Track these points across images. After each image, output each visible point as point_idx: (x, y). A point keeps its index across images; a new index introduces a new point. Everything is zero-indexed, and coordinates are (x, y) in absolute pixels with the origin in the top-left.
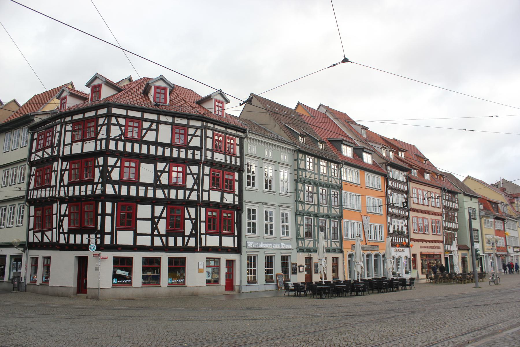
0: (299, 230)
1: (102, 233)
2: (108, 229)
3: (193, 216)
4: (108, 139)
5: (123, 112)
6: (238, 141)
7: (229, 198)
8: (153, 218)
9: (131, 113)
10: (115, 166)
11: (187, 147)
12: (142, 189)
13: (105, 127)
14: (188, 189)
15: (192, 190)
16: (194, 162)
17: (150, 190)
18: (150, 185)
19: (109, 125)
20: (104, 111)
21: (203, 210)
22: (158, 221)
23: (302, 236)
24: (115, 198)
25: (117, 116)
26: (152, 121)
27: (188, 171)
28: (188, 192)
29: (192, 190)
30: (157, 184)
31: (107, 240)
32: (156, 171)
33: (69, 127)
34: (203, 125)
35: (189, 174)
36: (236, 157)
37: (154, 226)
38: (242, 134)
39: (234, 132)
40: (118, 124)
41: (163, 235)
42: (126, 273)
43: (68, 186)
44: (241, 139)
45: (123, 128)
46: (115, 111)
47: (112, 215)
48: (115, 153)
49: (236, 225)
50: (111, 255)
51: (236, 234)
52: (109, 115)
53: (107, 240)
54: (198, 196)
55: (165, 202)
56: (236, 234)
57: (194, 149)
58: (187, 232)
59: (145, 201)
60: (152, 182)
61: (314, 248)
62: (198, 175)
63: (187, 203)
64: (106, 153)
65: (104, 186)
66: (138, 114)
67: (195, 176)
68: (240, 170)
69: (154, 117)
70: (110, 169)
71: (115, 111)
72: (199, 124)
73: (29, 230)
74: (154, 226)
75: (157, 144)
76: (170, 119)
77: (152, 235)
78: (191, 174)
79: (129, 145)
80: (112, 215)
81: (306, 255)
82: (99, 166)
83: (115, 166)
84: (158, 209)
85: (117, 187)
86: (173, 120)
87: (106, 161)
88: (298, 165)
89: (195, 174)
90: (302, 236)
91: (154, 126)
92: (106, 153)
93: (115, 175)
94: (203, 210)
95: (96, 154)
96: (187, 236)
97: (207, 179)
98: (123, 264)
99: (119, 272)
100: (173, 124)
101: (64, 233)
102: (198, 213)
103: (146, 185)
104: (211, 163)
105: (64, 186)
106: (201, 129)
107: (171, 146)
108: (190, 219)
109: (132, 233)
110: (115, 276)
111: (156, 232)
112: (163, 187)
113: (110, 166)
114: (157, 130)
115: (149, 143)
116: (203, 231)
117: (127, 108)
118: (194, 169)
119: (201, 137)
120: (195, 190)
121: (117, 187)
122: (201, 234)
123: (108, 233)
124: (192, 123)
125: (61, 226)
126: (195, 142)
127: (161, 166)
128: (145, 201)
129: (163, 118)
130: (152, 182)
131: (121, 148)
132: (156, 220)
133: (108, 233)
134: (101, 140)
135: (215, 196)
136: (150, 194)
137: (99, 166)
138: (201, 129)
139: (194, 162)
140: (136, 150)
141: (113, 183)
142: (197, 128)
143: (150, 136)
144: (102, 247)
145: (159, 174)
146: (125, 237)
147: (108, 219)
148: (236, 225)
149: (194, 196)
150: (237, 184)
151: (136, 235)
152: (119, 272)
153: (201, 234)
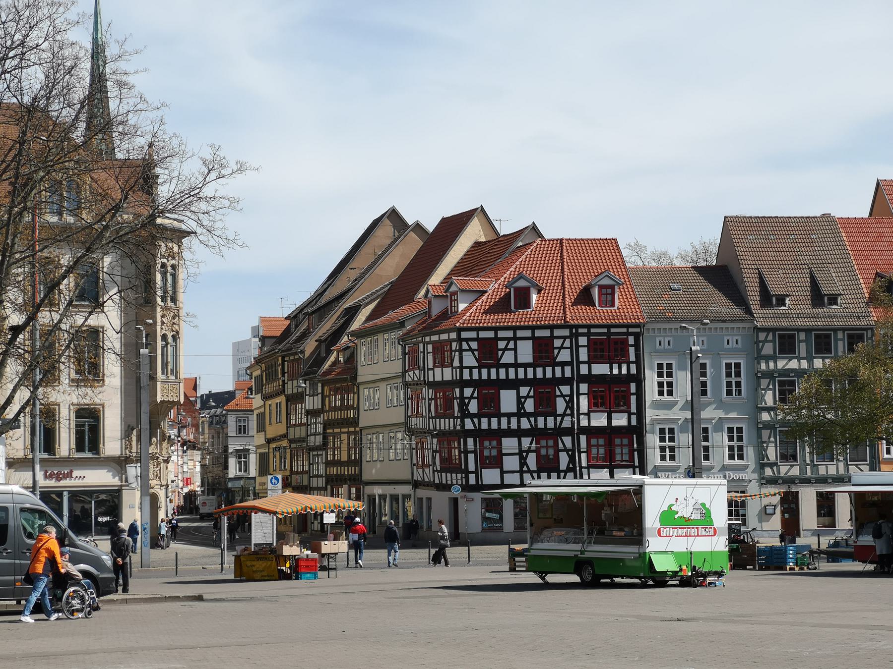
0: (766, 450)
1: (467, 472)
2: (472, 467)
3: (569, 445)
4: (462, 368)
5: (473, 335)
6: (631, 340)
7: (620, 420)
8: (520, 453)
9: (483, 334)
10: (472, 397)
11: (554, 364)
12: (504, 421)
13: (457, 353)
14: (559, 415)
15: (564, 415)
16: (564, 381)
17: (514, 420)
18: (513, 415)
19: (461, 351)
20: (453, 335)
21: (583, 439)
22: (527, 455)
23: (772, 459)
24: (477, 433)
25: (467, 340)
26: (508, 339)
27: (558, 393)
28: (559, 419)
29: (564, 415)
30: (520, 413)
31: (472, 480)
32: (519, 398)
33: (430, 348)
34: (571, 332)
35: (559, 396)
36: (629, 363)
37: (523, 462)
38: (638, 330)
39: (625, 330)
40: (472, 351)
41: (534, 472)
42: (495, 516)
43: (435, 418)
44: (637, 336)
45: (476, 353)
46: (464, 335)
47: (474, 452)
48: (470, 383)
49: (636, 453)
50: (478, 496)
51: (637, 464)
52: (460, 340)
53: (472, 480)
54: (573, 423)
55: (533, 432)
56: (637, 464)
57: (563, 364)
58: (563, 466)
59: (509, 433)
60: (514, 410)
61: (802, 476)
62: (571, 396)
63: (559, 432)
64: (463, 384)
65: (463, 422)
66: (490, 334)
67: (567, 399)
68: (639, 379)
69: (510, 334)
70: (467, 401)
71: (464, 335)
72: (566, 332)
73: (413, 465)
74: (523, 462)
75: (516, 365)
76: (528, 333)
77: (521, 472)
78: (562, 396)
79: (484, 371)
80: (474, 452)
81: (783, 489)
82: (457, 398)
83: (472, 397)
84: (526, 442)
85: (476, 420)
86: (533, 333)
87: (462, 392)
88: (759, 351)
89: (567, 396)
90: (772, 459)
91: (511, 345)
92: (463, 384)
93: (473, 407)
94: (583, 439)
95: (452, 384)
96: (563, 471)
97: (584, 402)
98: (493, 505)
99: (487, 515)
100: (533, 338)
101: (438, 472)
102: (576, 443)
103: (509, 415)
104: (589, 379)
105: (432, 418)
106: (570, 337)
107: (534, 365)
108: (566, 450)
109: (497, 471)
110: (484, 519)
111: (525, 469)
112: (528, 415)
113: (467, 398)
114: (515, 349)
115: (507, 366)
116: (584, 464)
117: (478, 329)
118: (565, 390)
119: (571, 348)
120: (568, 415)
121: (476, 420)
122: (581, 468)
123: (472, 472)
124: (557, 333)
125: (434, 463)
126: (564, 356)
127: (524, 391)
128: (509, 433)
129: (520, 334)
130: (514, 410)
131: (476, 376)
132: (524, 454)
133: (472, 472)
134: (456, 368)
135: (600, 420)
136: (514, 425)
137: (457, 398)
138: (570, 337)
139: (564, 381)
140: (493, 376)
141: (472, 416)
142: (565, 338)
143: (508, 358)
144: (467, 488)
145: (523, 400)
146: (491, 476)
147: (471, 457)
148: (636, 453)
149: (567, 423)
150: (633, 399)
151: (503, 472)
152: (487, 515)
153: (581, 468)
